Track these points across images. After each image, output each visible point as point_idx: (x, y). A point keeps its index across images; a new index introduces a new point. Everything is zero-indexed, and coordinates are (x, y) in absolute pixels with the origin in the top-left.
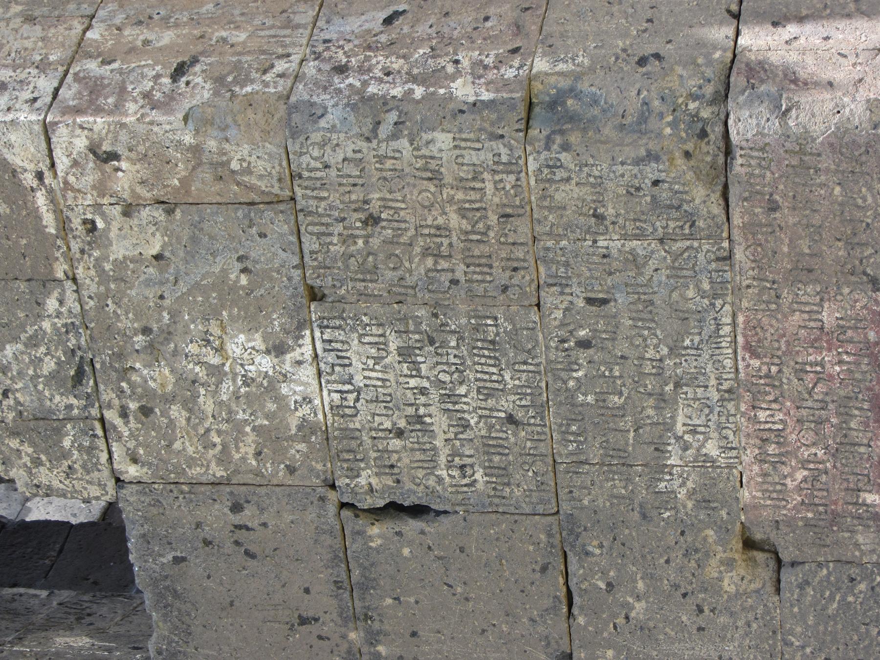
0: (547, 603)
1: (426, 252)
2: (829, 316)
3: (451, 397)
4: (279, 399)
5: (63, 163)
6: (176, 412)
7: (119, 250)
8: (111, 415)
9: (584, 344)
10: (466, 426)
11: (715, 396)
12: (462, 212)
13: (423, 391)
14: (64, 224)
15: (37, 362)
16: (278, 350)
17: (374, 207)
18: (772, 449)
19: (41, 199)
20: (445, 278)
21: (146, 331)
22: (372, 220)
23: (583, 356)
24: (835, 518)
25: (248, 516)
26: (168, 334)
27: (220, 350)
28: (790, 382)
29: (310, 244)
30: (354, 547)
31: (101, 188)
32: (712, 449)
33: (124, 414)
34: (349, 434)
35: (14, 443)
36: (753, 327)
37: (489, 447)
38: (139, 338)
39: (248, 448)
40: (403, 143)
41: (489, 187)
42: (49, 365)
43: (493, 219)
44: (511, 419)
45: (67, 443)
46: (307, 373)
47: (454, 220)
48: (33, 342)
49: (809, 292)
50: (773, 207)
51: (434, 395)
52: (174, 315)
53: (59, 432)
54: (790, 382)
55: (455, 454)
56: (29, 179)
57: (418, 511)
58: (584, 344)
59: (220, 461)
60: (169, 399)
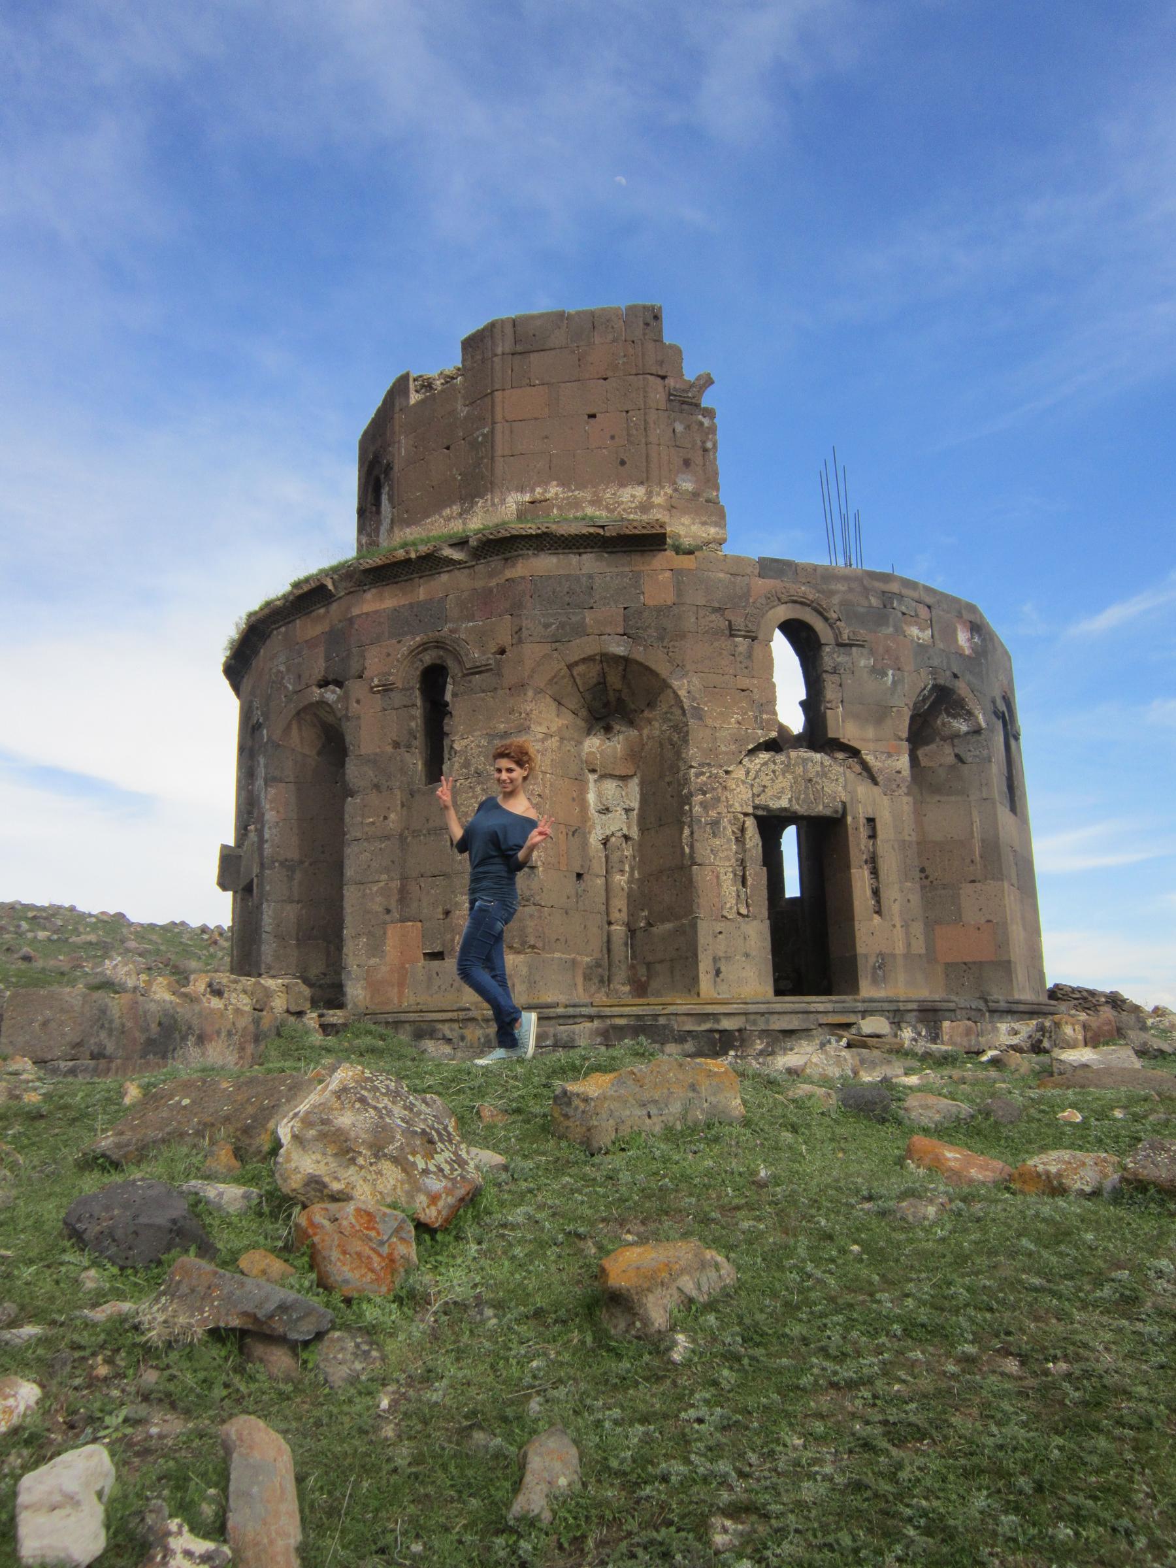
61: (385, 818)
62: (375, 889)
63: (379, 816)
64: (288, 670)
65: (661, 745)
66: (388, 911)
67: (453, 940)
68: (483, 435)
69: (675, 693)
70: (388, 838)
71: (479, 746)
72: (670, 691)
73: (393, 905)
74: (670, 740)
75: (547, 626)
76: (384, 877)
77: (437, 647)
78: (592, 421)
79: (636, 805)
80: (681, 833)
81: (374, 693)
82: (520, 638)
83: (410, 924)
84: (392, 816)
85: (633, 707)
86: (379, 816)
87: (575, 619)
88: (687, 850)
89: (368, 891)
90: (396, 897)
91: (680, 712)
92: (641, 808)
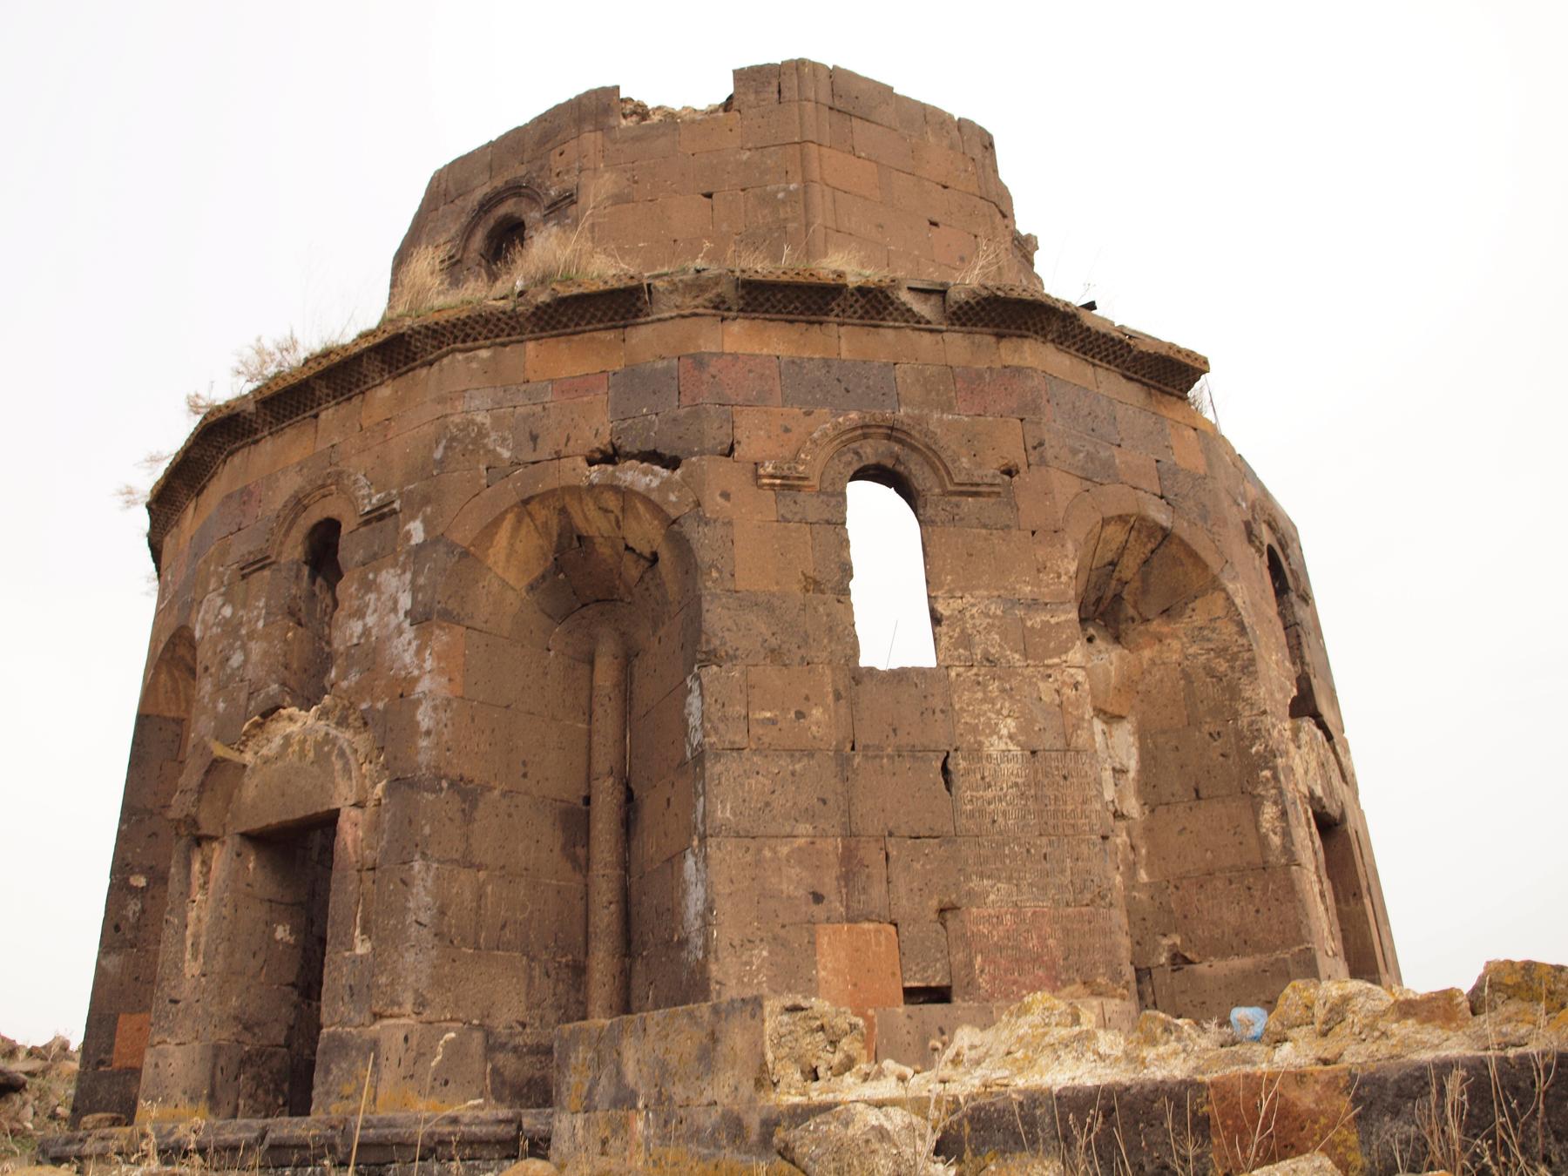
0: (916, 829)
1: (1056, 797)
2: (1051, 942)
3: (1000, 800)
4: (991, 735)
5: (1072, 671)
6: (980, 695)
7: (1041, 685)
8: (975, 670)
9: (1028, 851)
10: (989, 804)
11: (1014, 899)
12: (1073, 811)
13: (1002, 789)
14: (1048, 666)
15: (993, 646)
16: (1011, 737)
17: (1070, 779)
18: (995, 920)
19: (1056, 660)
20: (1047, 802)
21: (1011, 689)
22: (1065, 778)
23: (1024, 850)
24: (968, 945)
25: (939, 715)
26: (1011, 697)
27: (1009, 716)
28: (1023, 927)
29: (1054, 754)
30: (931, 755)
31: (1064, 683)
32: (992, 897)
33: (976, 675)
34: (980, 759)
35: (958, 630)
36: (1044, 914)
37: (982, 812)
38: (1008, 687)
39: (968, 719)
40: (1095, 793)
41: (1083, 821)
42: (993, 651)
43: (1072, 822)
44: (994, 822)
45: (961, 651)
46: (1002, 746)
47: (1069, 808)
48: (1000, 645)
49: (1059, 934)
50: (1090, 922)
51: (1001, 793)
52: (1019, 701)
53: (965, 648)
54: (1023, 927)
55: (977, 799)
56: (1064, 658)
57: (948, 784)
58: (1028, 851)
59: (961, 708)
60: (985, 692)
61: (800, 715)
62: (784, 850)
63: (785, 710)
64: (498, 422)
65: (1186, 676)
66: (818, 898)
67: (970, 964)
68: (789, 193)
69: (1229, 599)
70: (811, 755)
71: (987, 615)
72: (1219, 598)
73: (829, 883)
74: (1211, 672)
75: (1075, 452)
76: (804, 828)
77: (889, 437)
78: (933, 228)
79: (1133, 764)
80: (1256, 812)
81: (761, 487)
82: (1042, 457)
83: (866, 926)
84: (817, 713)
85: (1131, 612)
86: (785, 710)
87: (1104, 454)
88: (1276, 840)
89: (767, 853)
90: (835, 871)
91: (1233, 628)
92: (1144, 768)
